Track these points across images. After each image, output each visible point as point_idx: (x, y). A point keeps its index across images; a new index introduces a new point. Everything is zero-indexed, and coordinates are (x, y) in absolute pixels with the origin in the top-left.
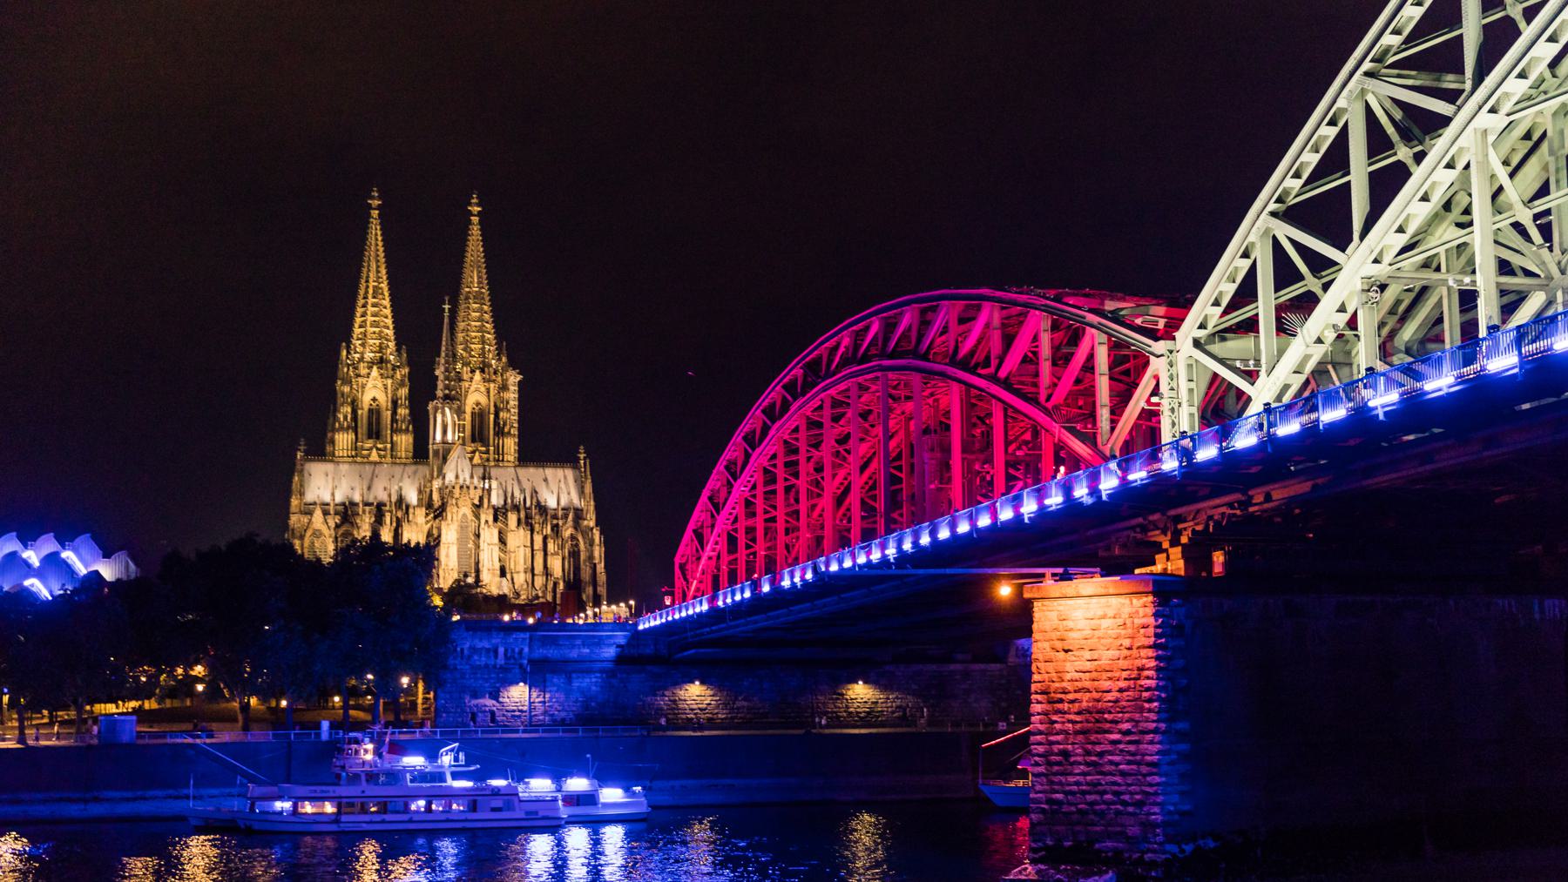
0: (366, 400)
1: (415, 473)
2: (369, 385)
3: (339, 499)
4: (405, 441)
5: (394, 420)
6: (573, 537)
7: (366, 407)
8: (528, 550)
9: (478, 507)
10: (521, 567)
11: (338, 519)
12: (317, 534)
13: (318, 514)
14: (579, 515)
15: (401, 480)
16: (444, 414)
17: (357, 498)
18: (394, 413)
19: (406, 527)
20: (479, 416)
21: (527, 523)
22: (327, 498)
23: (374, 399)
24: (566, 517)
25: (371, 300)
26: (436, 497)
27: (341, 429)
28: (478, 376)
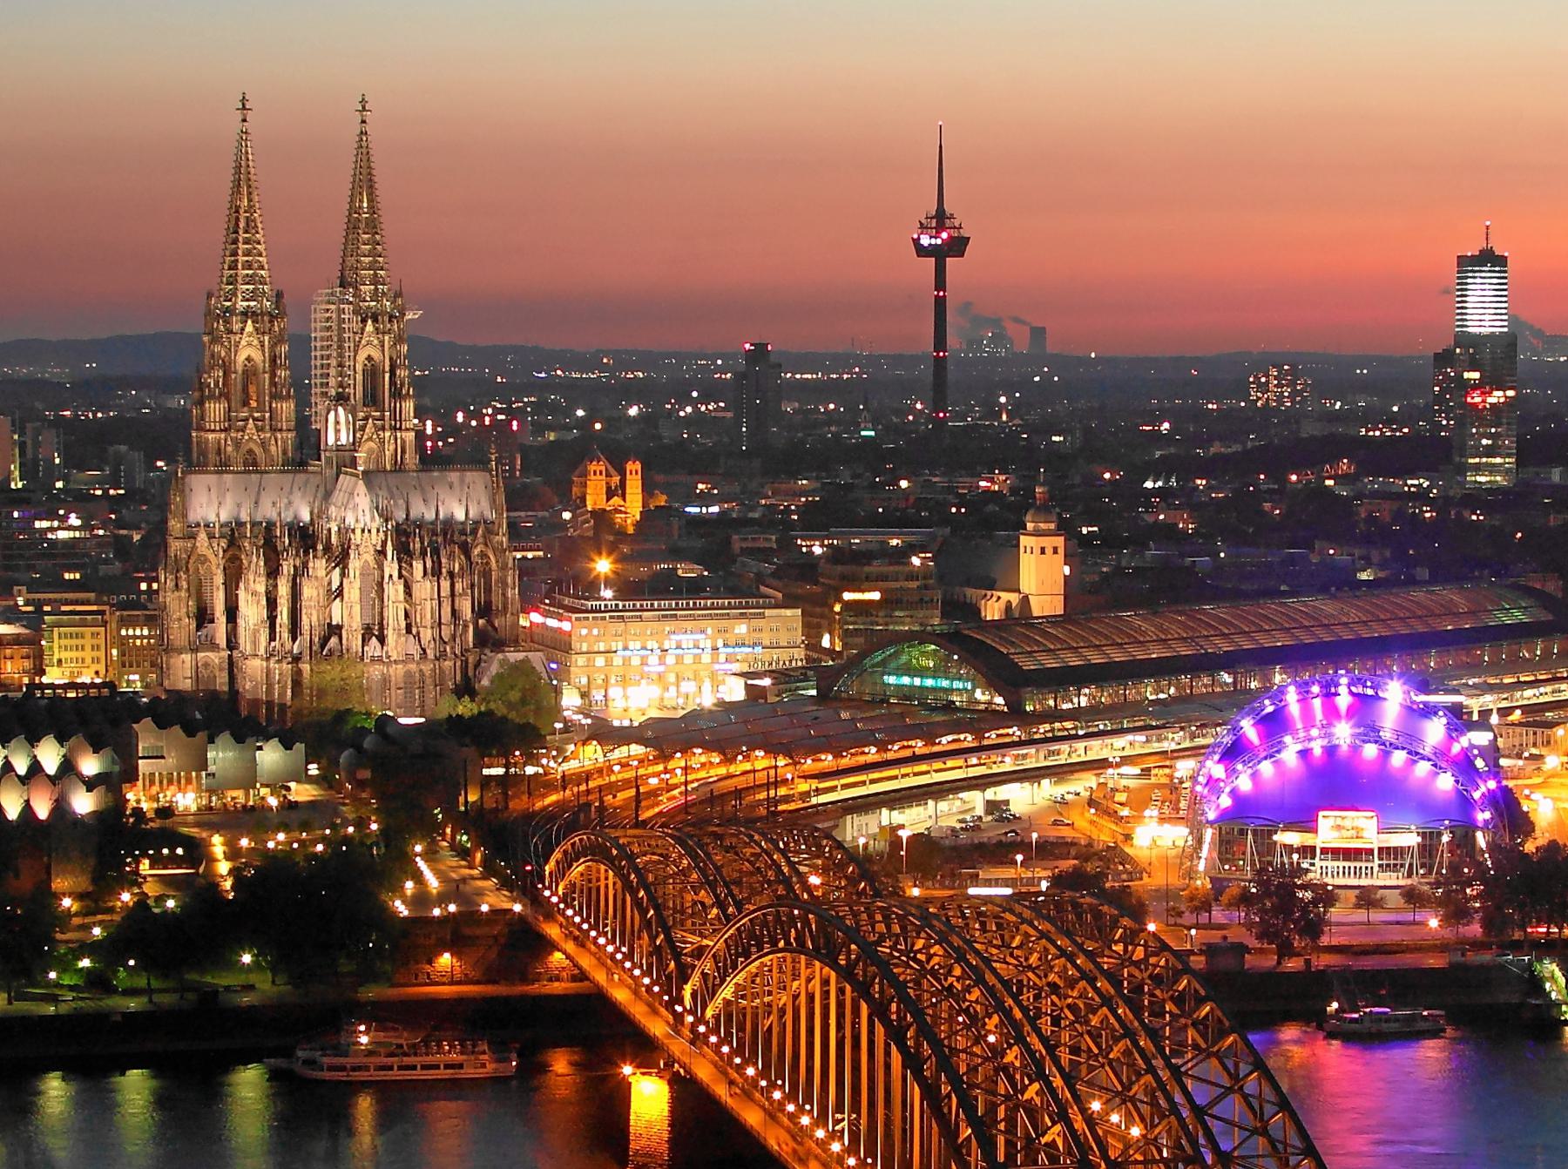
0: (241, 358)
1: (306, 482)
2: (243, 343)
3: (224, 517)
4: (286, 409)
5: (273, 384)
6: (483, 555)
7: (240, 369)
8: (435, 602)
9: (382, 553)
10: (428, 620)
11: (224, 543)
12: (204, 560)
13: (202, 536)
14: (490, 528)
15: (291, 493)
16: (336, 415)
17: (244, 517)
18: (273, 375)
19: (305, 581)
20: (372, 372)
21: (436, 572)
22: (212, 518)
23: (249, 359)
24: (474, 532)
25: (242, 236)
26: (334, 540)
27: (212, 397)
28: (369, 327)
